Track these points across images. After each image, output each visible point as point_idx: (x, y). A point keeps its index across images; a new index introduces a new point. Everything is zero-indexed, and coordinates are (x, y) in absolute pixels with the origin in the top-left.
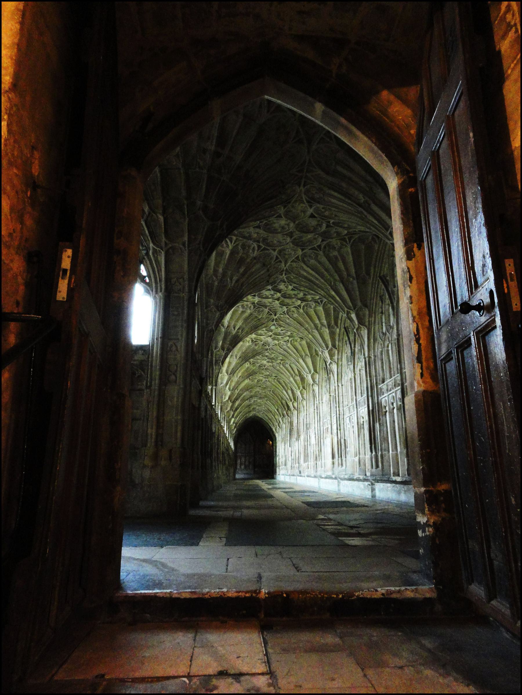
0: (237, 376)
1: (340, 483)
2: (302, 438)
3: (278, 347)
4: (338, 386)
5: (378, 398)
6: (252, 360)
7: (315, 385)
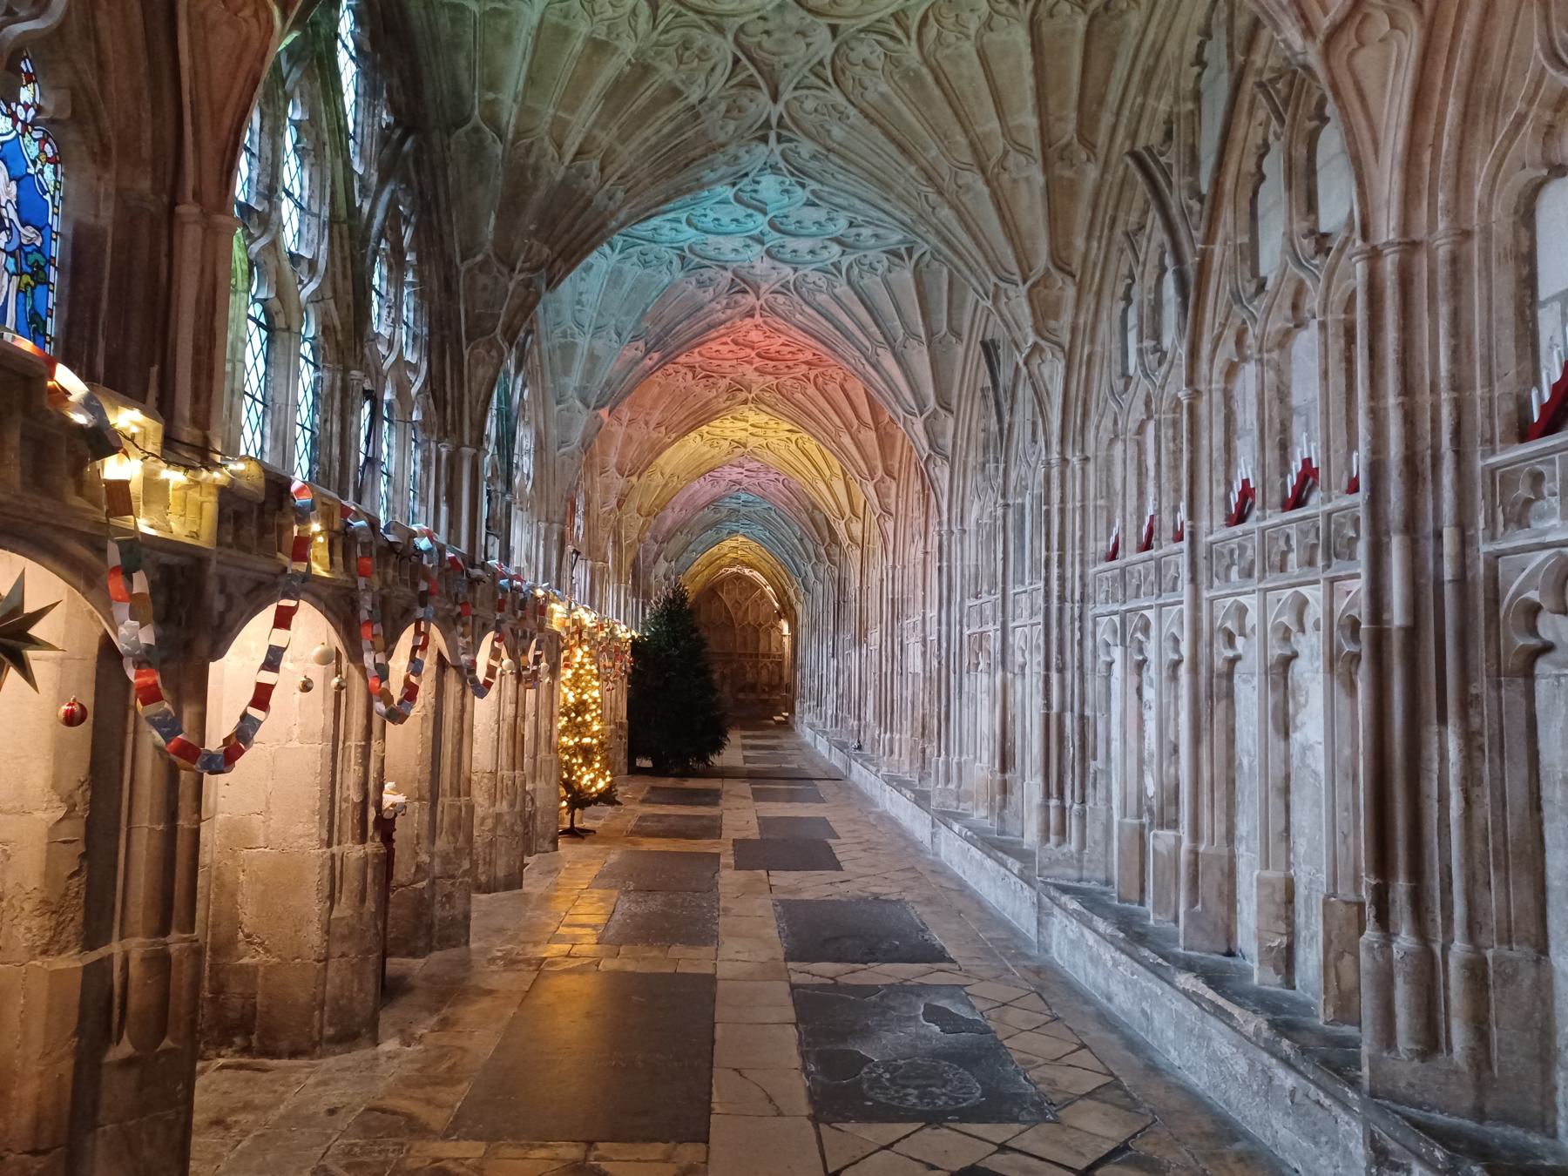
0: (647, 423)
1: (1050, 914)
2: (874, 637)
3: (796, 298)
4: (1064, 461)
5: (1464, 542)
6: (695, 358)
7: (939, 461)
